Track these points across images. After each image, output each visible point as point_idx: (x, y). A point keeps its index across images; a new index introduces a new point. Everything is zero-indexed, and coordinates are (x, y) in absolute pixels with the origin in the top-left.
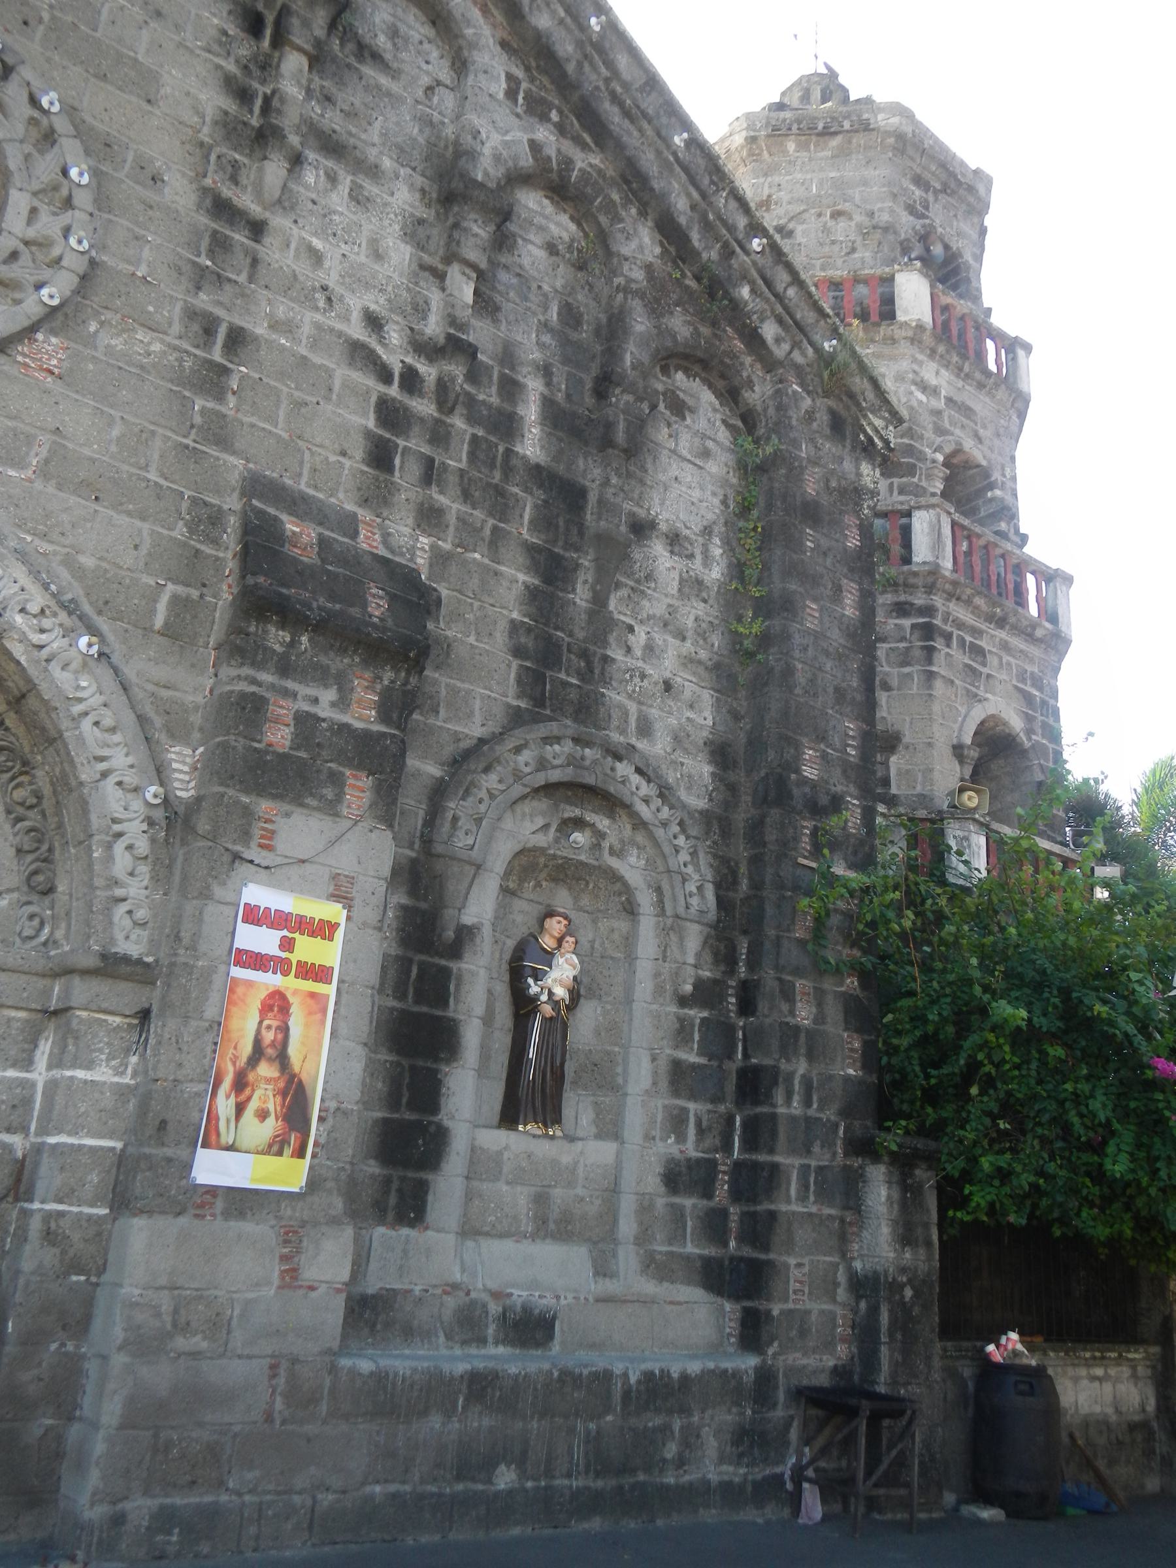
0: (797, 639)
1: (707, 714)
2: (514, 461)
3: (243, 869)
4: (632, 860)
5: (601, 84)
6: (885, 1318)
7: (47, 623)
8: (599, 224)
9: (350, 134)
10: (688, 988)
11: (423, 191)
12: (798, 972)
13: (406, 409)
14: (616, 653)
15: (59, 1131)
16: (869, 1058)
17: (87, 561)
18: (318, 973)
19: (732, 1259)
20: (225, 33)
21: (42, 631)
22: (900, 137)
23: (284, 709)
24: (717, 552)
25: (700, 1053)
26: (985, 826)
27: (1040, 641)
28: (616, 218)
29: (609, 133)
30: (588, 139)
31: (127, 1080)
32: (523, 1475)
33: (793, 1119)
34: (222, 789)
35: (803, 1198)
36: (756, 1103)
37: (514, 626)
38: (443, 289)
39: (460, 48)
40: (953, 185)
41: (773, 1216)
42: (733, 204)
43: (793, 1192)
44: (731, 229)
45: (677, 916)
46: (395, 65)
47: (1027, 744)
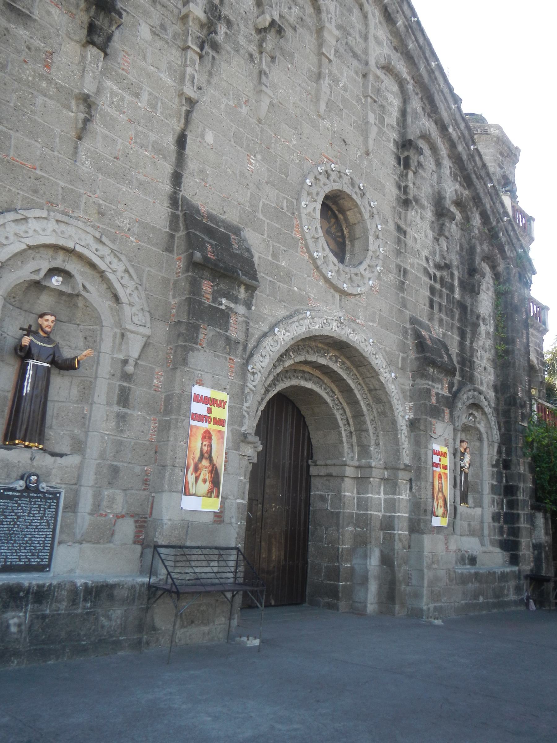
0: (516, 352)
1: (493, 376)
2: (455, 301)
3: (432, 439)
4: (482, 424)
5: (472, 168)
6: (543, 555)
7: (387, 370)
8: (467, 215)
9: (419, 195)
10: (495, 462)
11: (433, 211)
12: (520, 457)
13: (435, 287)
14: (475, 360)
15: (399, 512)
16: (534, 482)
17: (388, 349)
18: (445, 467)
19: (505, 540)
20: (394, 166)
21: (386, 373)
22: (498, 138)
23: (433, 392)
24: (492, 322)
25: (496, 482)
26: (536, 401)
27: (541, 331)
28: (472, 213)
29: (474, 185)
30: (465, 185)
31: (407, 498)
32: (484, 599)
33: (521, 500)
34: (426, 417)
35: (524, 523)
36: (513, 495)
37: (457, 353)
38: (439, 245)
39: (439, 159)
40: (510, 154)
41: (519, 528)
42: (500, 205)
43: (522, 521)
44: (499, 214)
45: (493, 441)
46: (425, 167)
47: (538, 368)
